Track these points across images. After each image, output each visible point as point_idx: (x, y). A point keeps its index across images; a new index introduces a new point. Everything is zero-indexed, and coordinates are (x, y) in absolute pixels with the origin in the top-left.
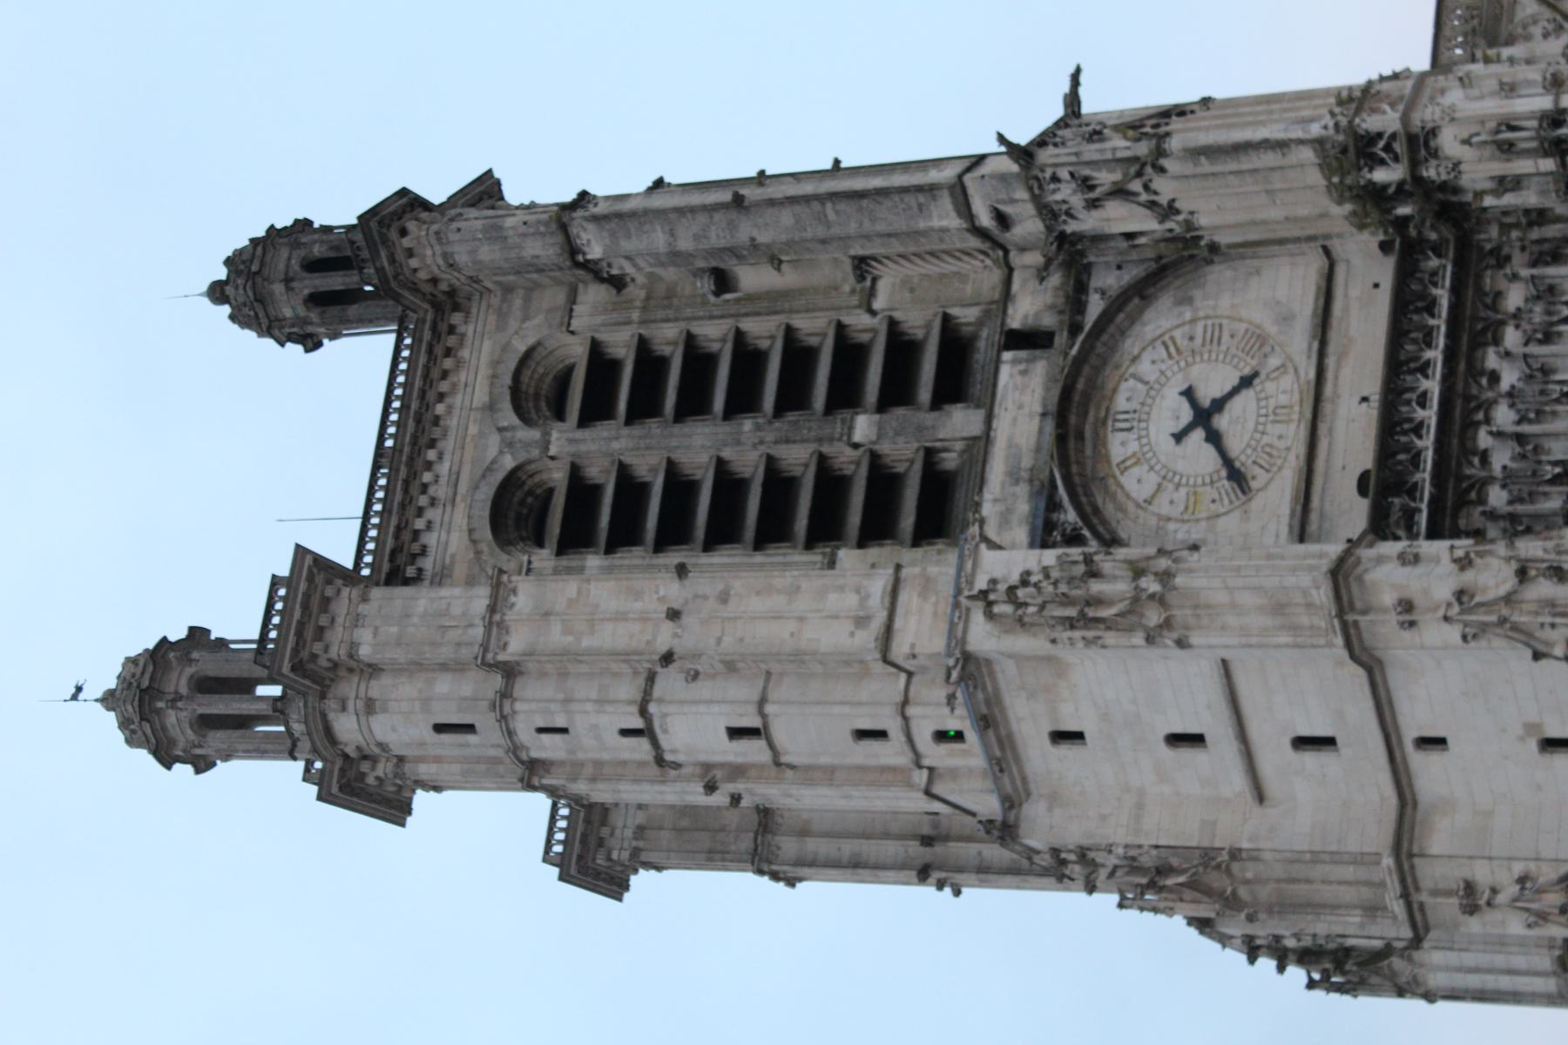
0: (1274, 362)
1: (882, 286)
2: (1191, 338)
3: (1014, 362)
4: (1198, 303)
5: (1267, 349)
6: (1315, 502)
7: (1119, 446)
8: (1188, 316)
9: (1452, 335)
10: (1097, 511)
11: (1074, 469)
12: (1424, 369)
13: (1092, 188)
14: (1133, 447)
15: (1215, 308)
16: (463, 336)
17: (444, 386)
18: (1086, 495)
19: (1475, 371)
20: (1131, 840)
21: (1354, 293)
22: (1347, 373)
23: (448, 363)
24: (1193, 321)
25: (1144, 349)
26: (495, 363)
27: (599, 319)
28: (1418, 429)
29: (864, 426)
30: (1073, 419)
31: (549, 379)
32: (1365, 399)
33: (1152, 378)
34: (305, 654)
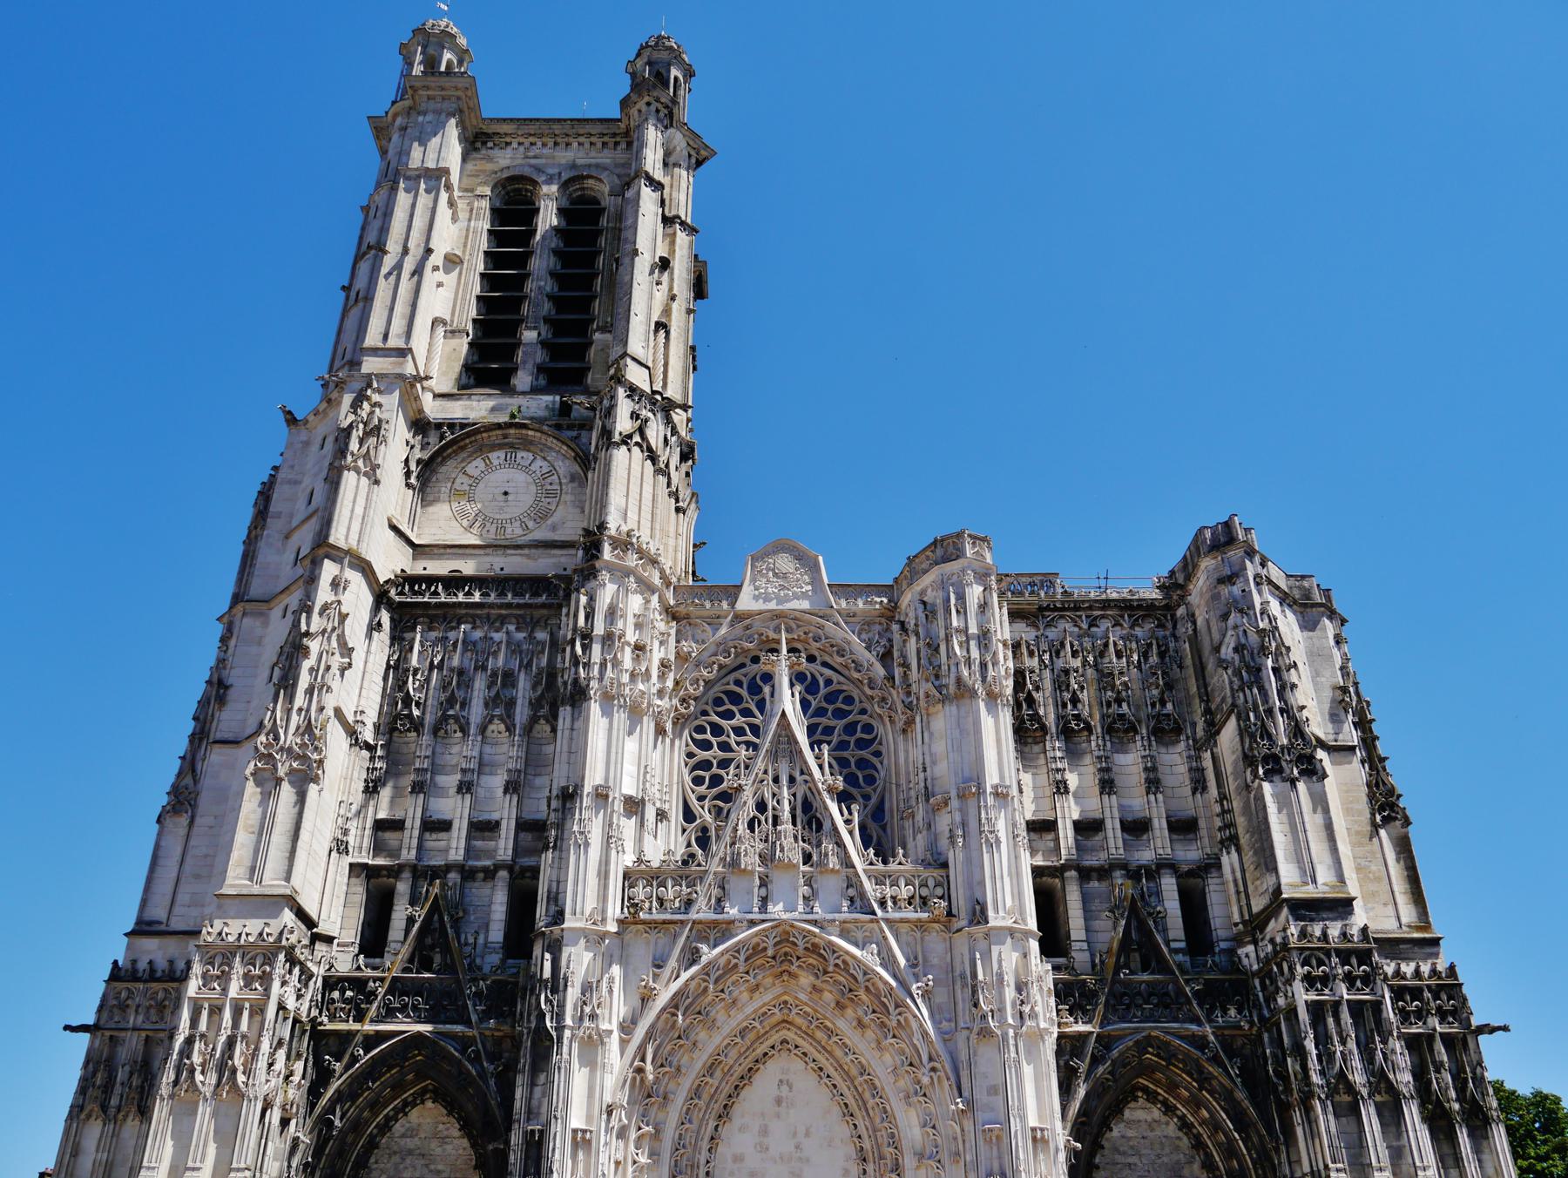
0: (531, 524)
1: (608, 337)
2: (551, 484)
3: (554, 402)
4: (570, 485)
5: (538, 520)
6: (448, 551)
7: (497, 457)
8: (564, 481)
9: (519, 606)
10: (463, 448)
11: (484, 435)
12: (502, 594)
13: (606, 417)
14: (496, 462)
15: (566, 493)
16: (615, 149)
17: (587, 145)
18: (471, 443)
19: (503, 620)
20: (279, 480)
21: (563, 560)
22: (518, 559)
23: (599, 145)
24: (560, 483)
25: (549, 462)
26: (597, 166)
27: (612, 209)
28: (469, 594)
29: (529, 336)
30: (512, 431)
31: (593, 194)
32: (502, 569)
33: (533, 468)
34: (421, 92)
